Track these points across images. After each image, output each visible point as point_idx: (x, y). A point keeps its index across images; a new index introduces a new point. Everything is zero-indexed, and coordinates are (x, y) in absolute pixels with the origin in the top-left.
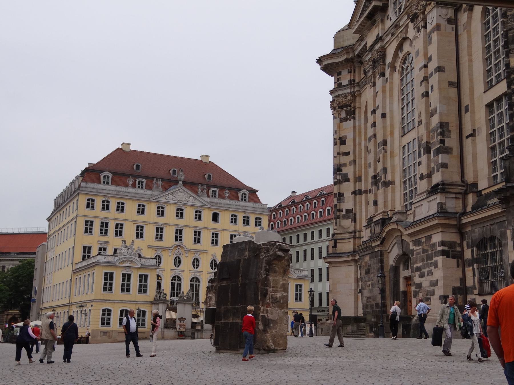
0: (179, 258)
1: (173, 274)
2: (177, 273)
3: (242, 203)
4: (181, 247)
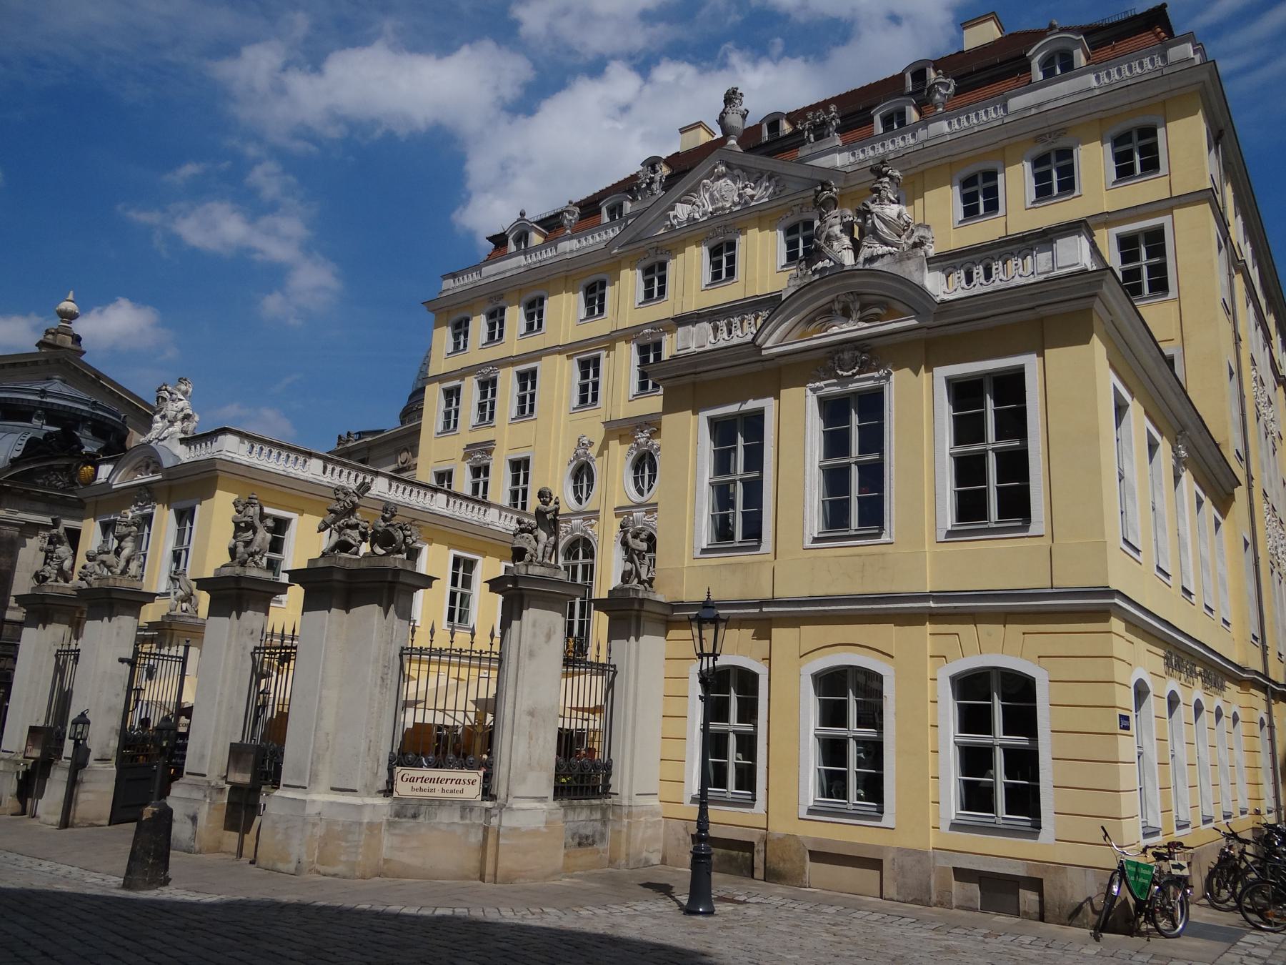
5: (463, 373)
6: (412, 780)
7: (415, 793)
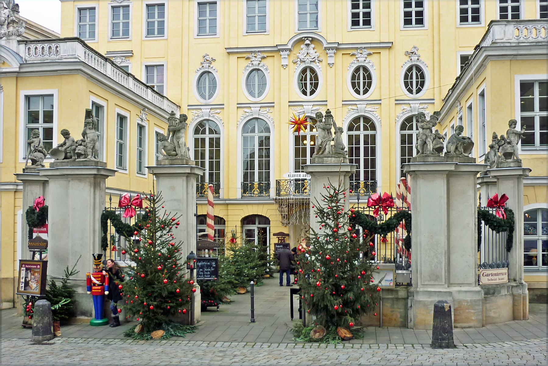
0: (312, 71)
4: (313, 40)
6: (487, 275)
7: (489, 282)
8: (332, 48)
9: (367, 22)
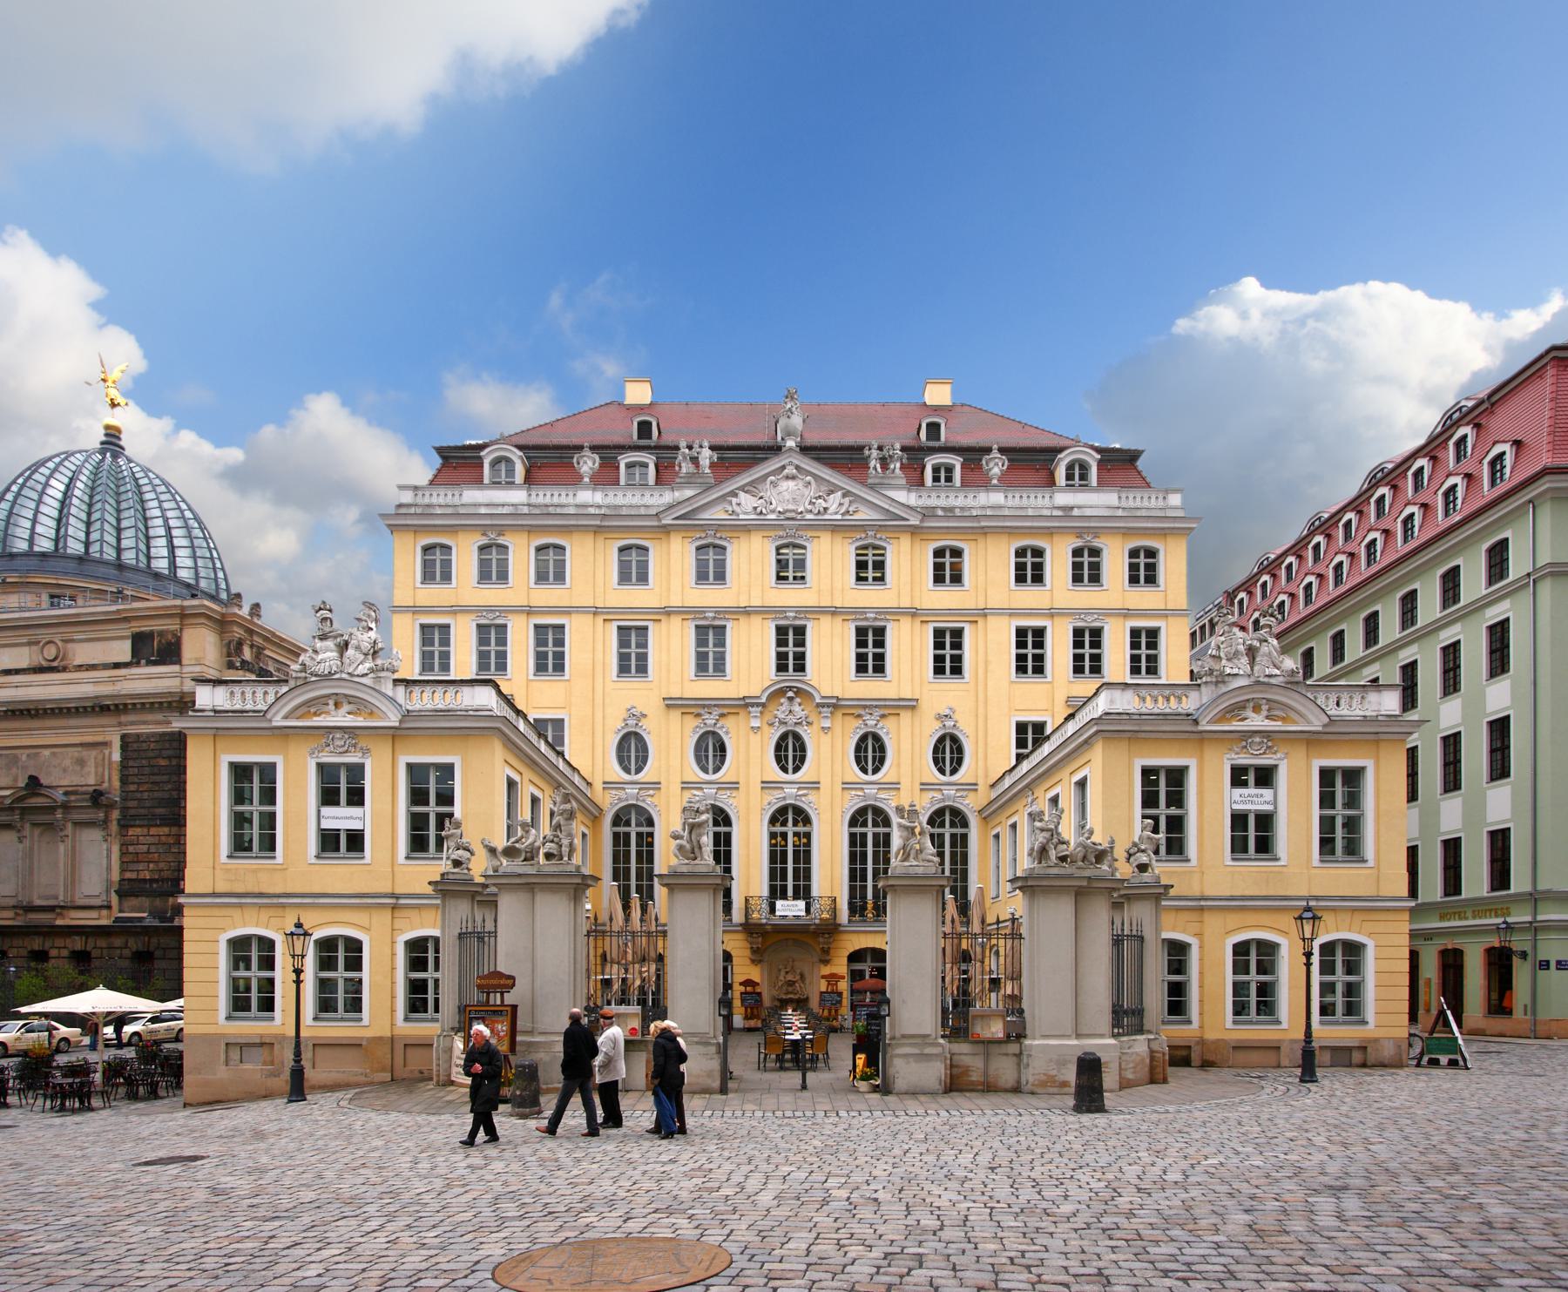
0: (797, 737)
1: (773, 800)
2: (790, 794)
3: (1063, 498)
4: (799, 692)
5: (455, 610)
8: (828, 706)
9: (880, 669)
